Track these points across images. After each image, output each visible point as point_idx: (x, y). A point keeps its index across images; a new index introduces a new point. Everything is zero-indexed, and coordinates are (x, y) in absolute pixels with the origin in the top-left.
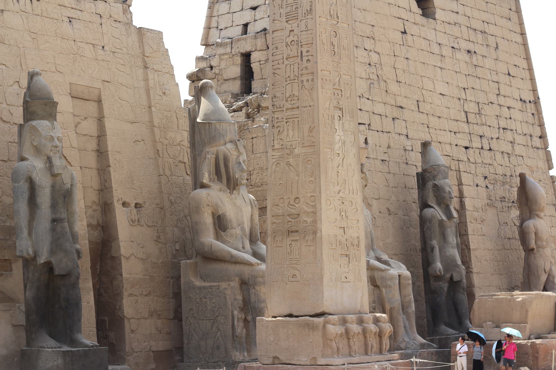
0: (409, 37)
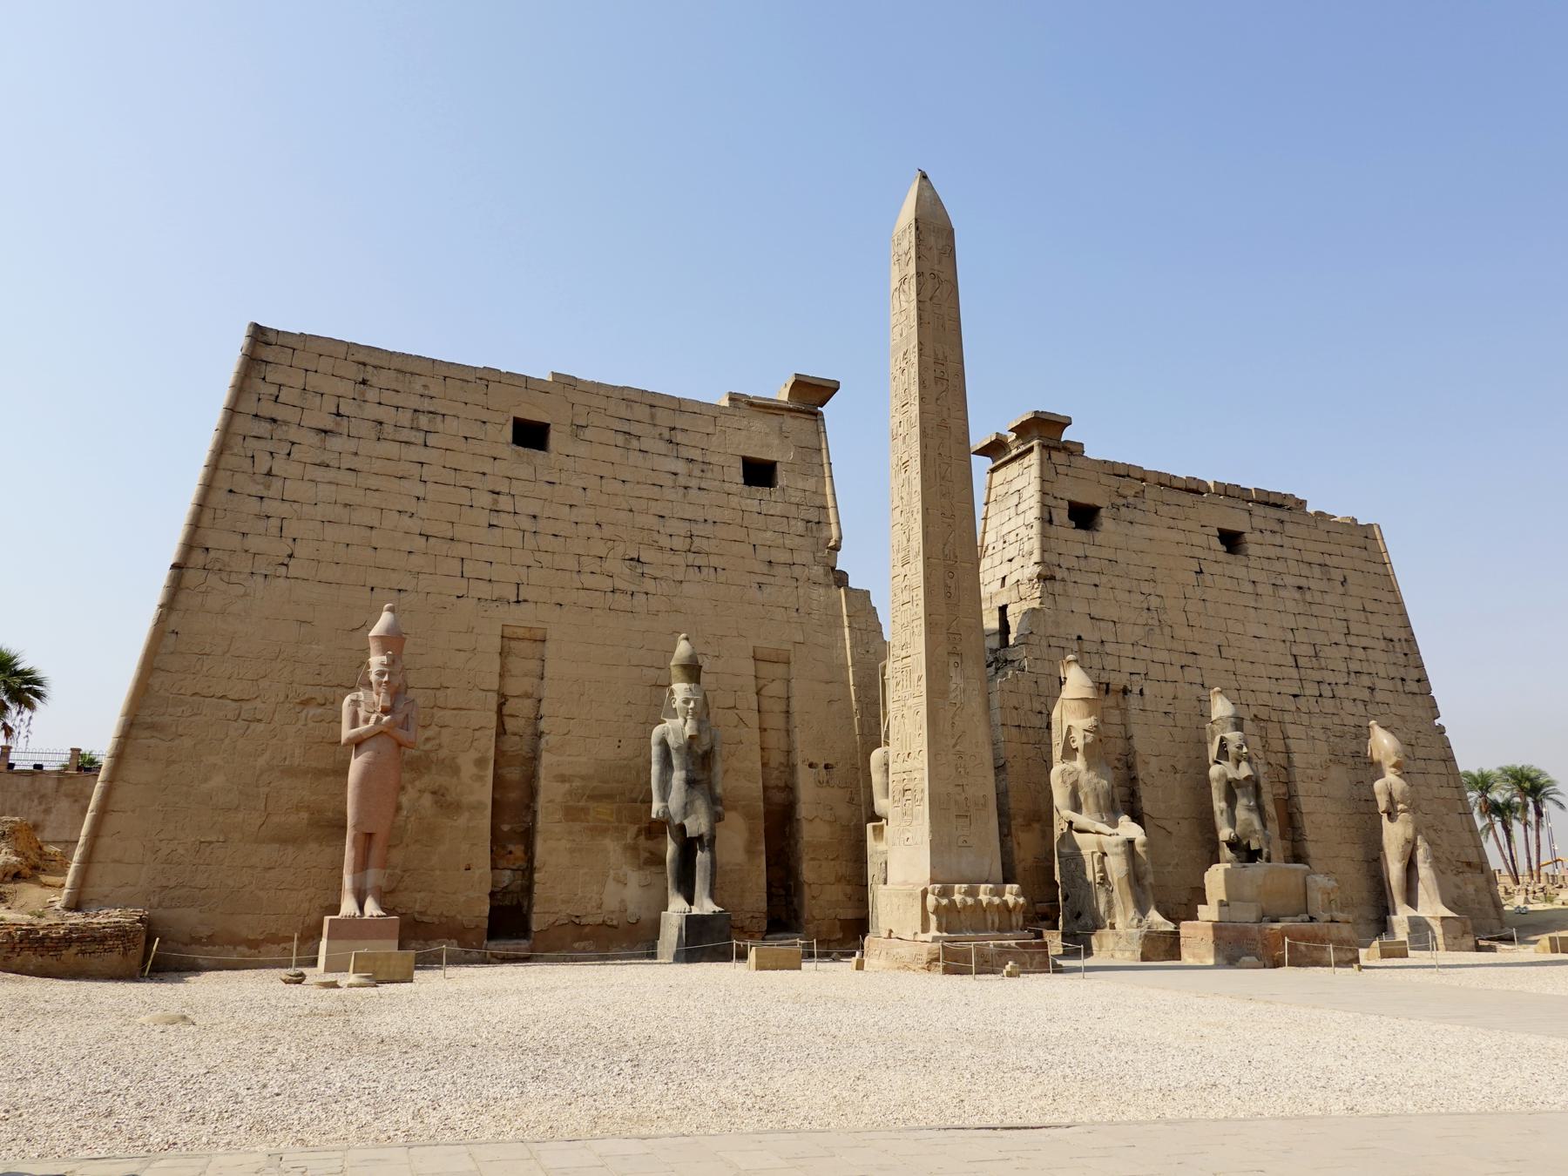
0: (1207, 577)
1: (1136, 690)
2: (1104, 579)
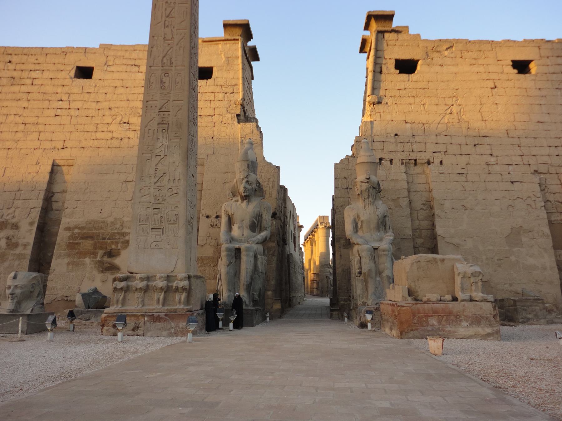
1: (437, 161)
2: (418, 100)
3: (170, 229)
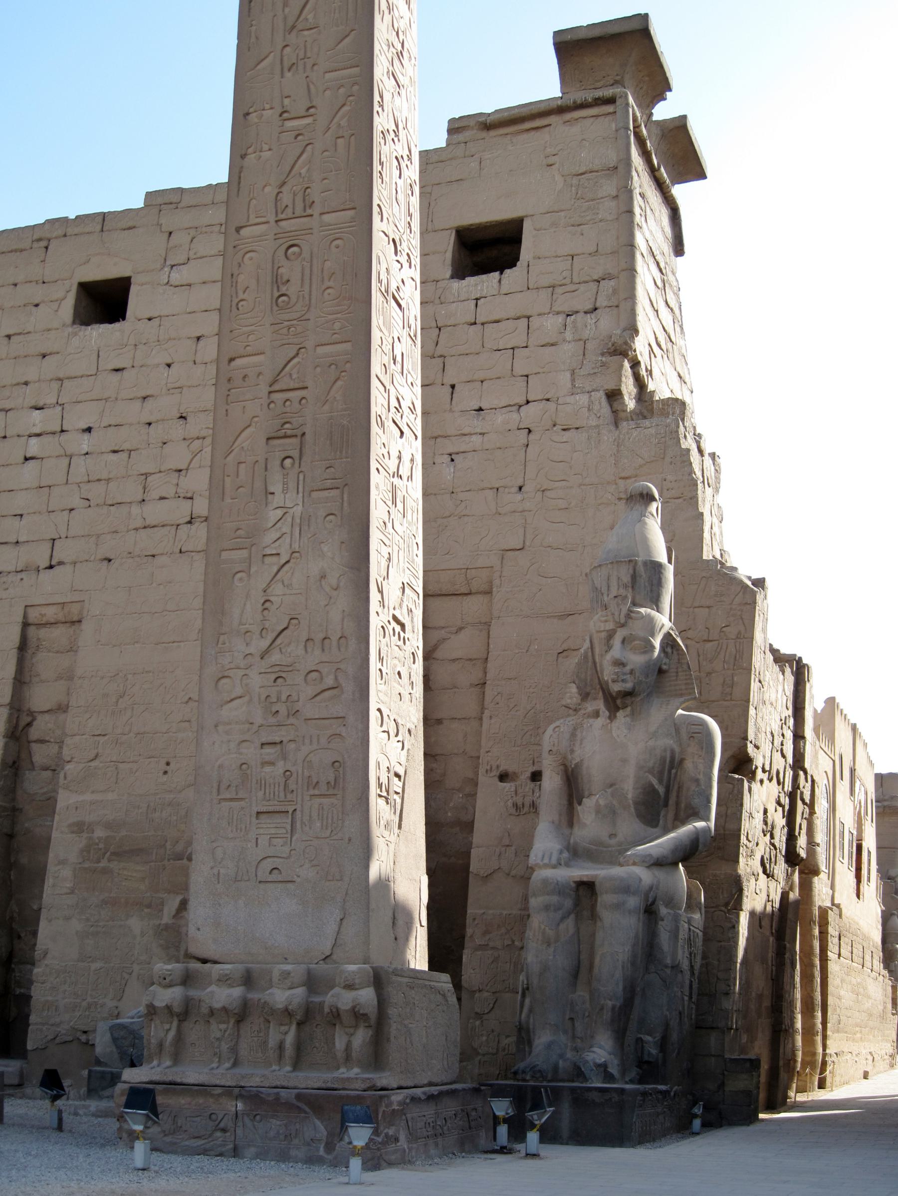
3: (315, 815)
